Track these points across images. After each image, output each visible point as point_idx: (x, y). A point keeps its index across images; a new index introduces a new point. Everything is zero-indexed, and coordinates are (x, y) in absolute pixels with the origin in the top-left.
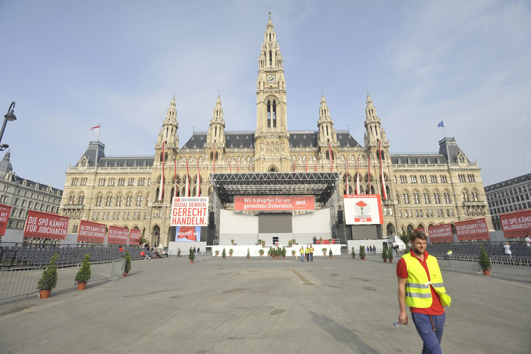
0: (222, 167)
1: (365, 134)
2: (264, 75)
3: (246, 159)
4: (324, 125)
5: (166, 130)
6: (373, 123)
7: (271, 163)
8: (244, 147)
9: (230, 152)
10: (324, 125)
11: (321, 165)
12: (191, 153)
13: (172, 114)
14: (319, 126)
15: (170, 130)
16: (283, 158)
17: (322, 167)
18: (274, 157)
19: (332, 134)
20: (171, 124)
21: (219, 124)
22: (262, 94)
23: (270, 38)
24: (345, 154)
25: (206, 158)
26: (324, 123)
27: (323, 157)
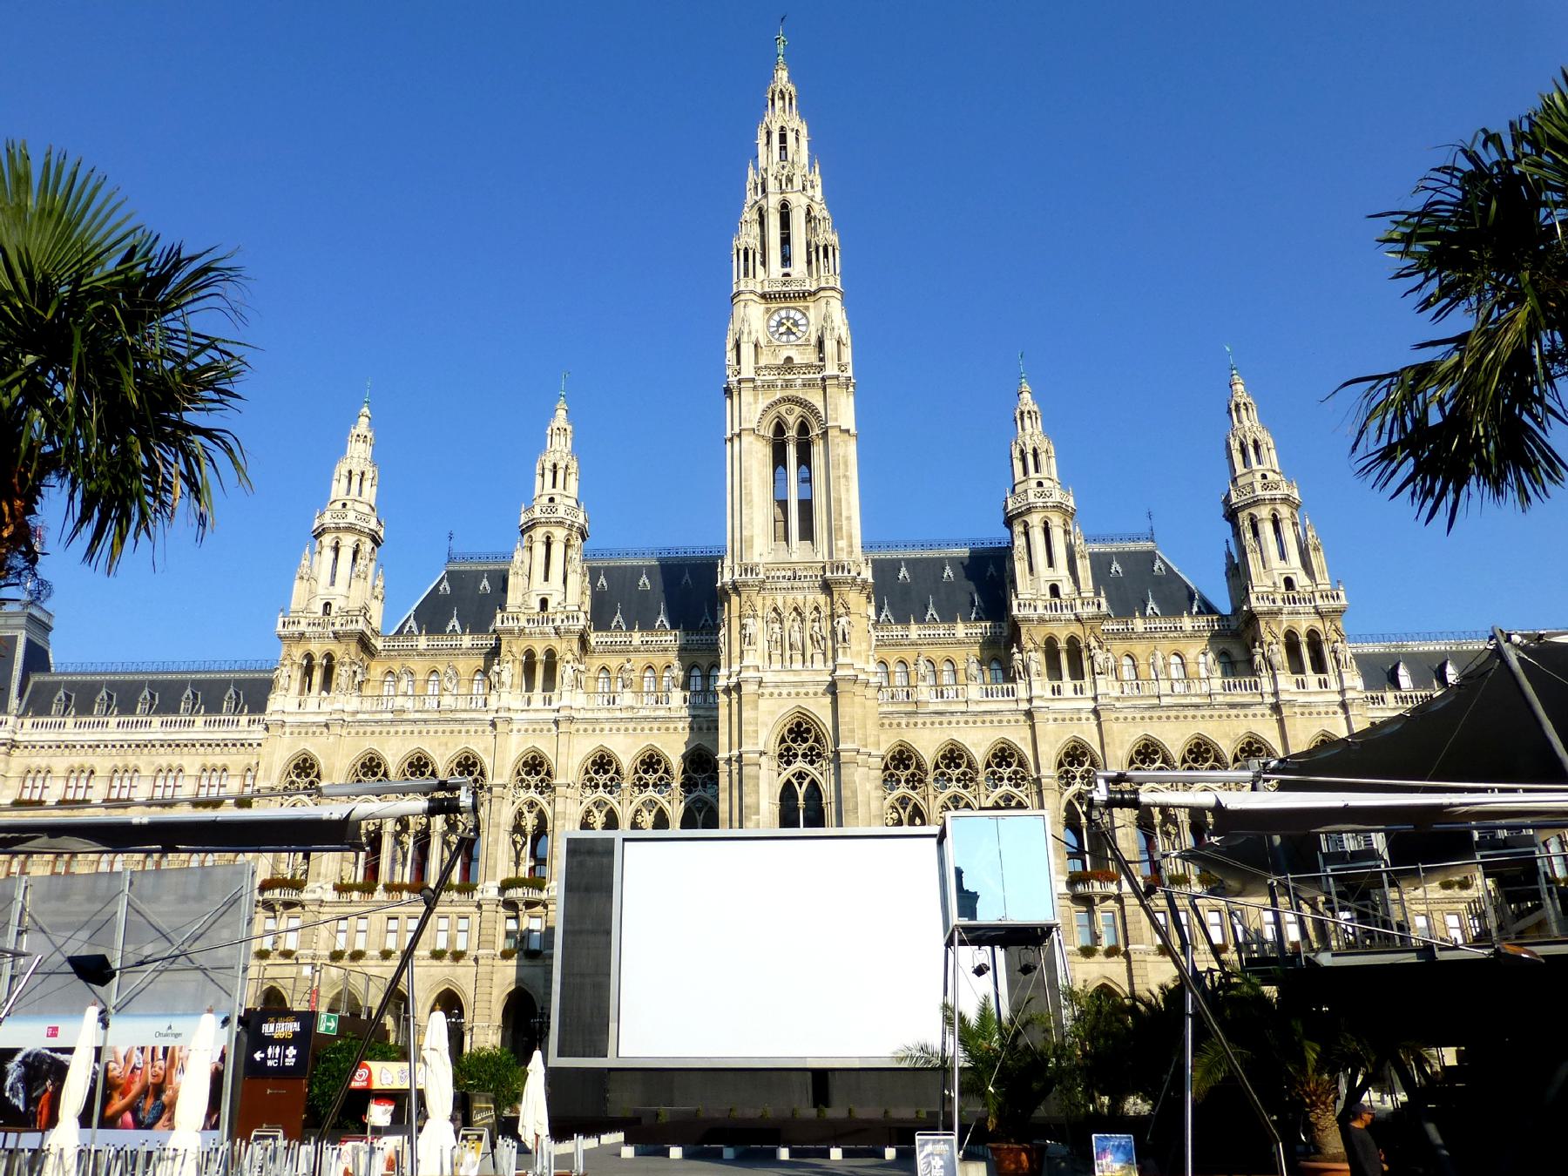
0: (571, 720)
1: (1229, 556)
4: (1035, 520)
5: (328, 555)
9: (610, 649)
11: (1024, 706)
12: (433, 652)
13: (356, 480)
14: (1009, 522)
15: (346, 554)
16: (843, 679)
18: (805, 677)
20: (350, 529)
21: (560, 523)
23: (783, 148)
24: (1139, 649)
25: (505, 677)
27: (1033, 667)
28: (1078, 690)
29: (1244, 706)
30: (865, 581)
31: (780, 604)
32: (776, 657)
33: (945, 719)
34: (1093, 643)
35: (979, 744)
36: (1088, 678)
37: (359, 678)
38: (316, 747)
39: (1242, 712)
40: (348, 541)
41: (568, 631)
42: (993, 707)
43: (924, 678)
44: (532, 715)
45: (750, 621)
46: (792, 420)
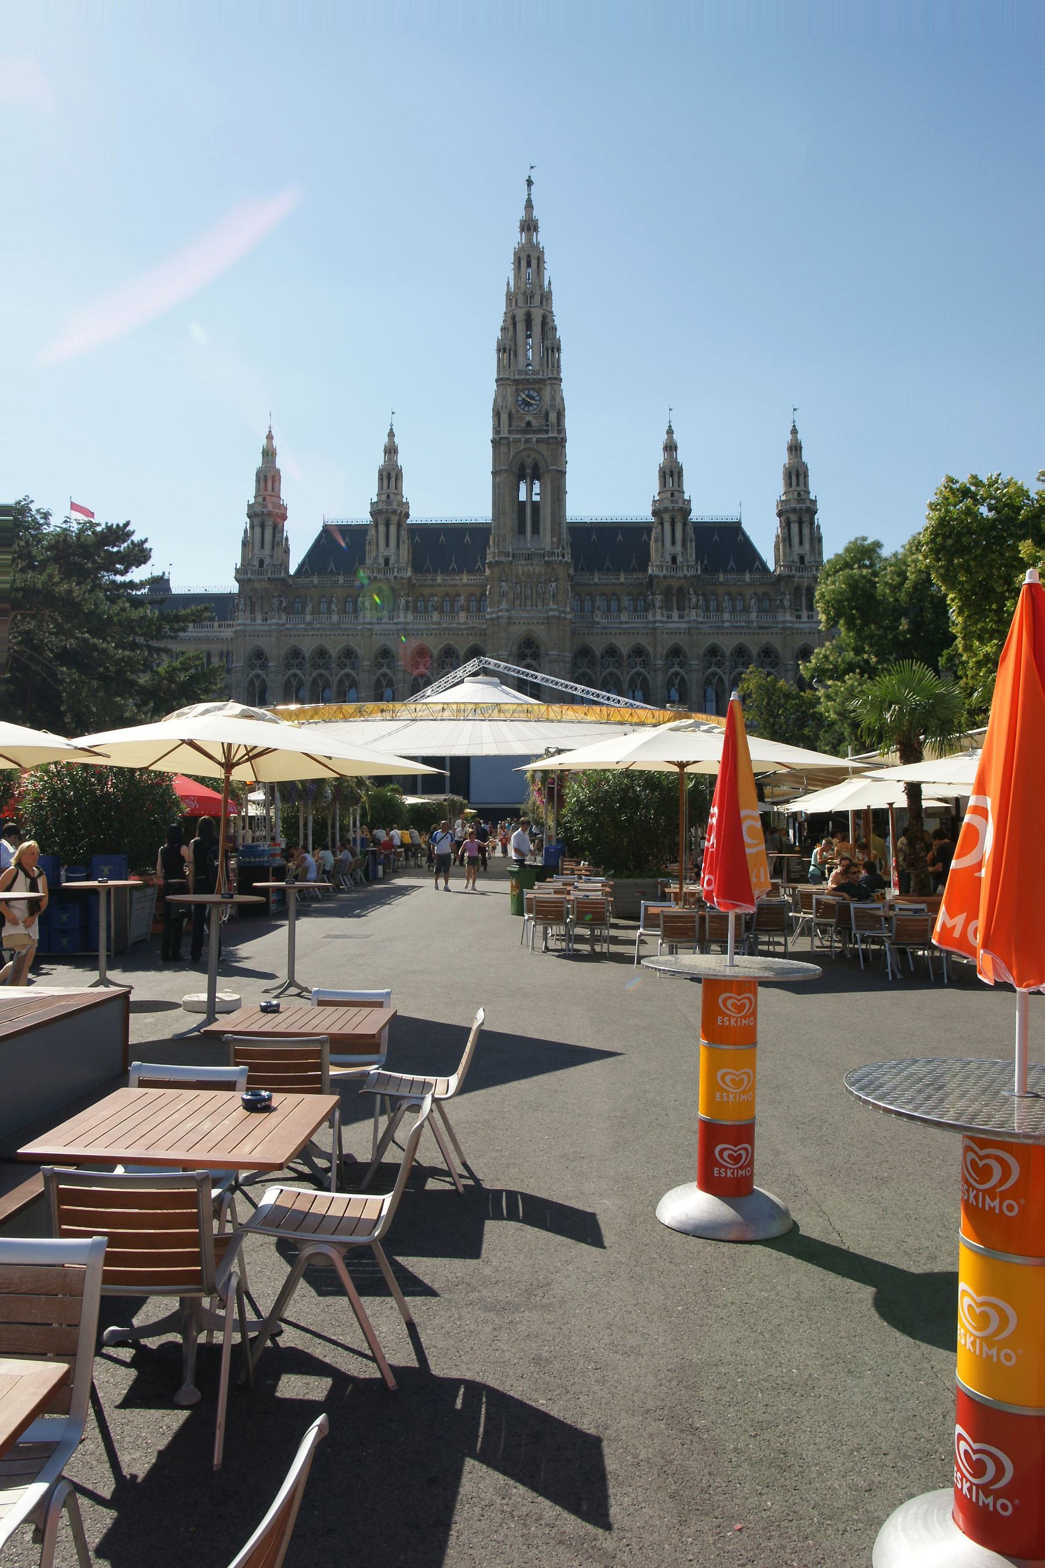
0: (405, 629)
1: (778, 537)
2: (510, 390)
3: (462, 609)
5: (258, 530)
6: (794, 510)
7: (524, 628)
8: (461, 572)
10: (667, 517)
11: (650, 625)
16: (552, 617)
17: (654, 629)
19: (684, 540)
22: (504, 449)
26: (666, 510)
27: (658, 604)
28: (681, 617)
29: (766, 628)
30: (566, 563)
31: (520, 572)
32: (517, 603)
33: (608, 631)
34: (692, 592)
35: (624, 646)
36: (687, 611)
37: (284, 604)
38: (262, 643)
39: (765, 631)
40: (269, 523)
41: (402, 578)
42: (635, 625)
43: (599, 609)
44: (383, 626)
45: (503, 584)
46: (529, 460)
